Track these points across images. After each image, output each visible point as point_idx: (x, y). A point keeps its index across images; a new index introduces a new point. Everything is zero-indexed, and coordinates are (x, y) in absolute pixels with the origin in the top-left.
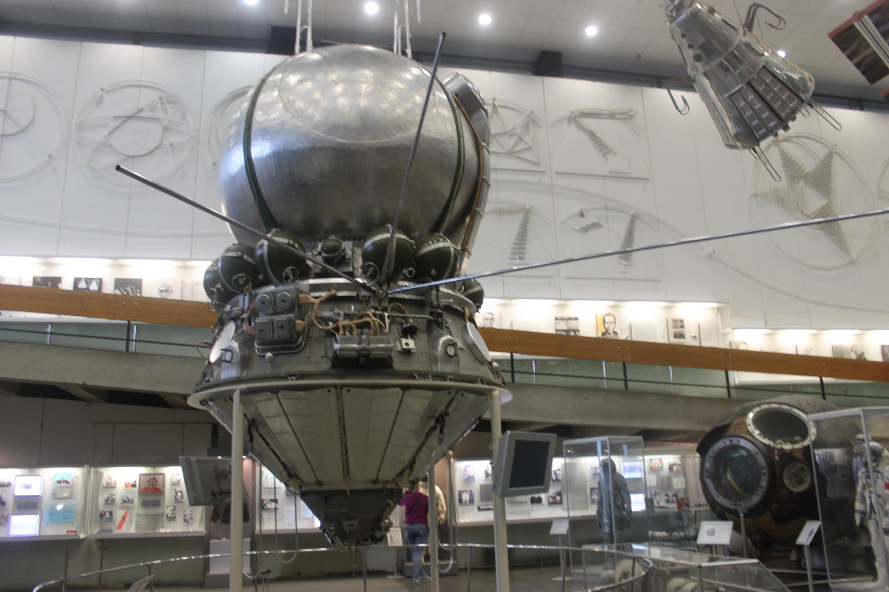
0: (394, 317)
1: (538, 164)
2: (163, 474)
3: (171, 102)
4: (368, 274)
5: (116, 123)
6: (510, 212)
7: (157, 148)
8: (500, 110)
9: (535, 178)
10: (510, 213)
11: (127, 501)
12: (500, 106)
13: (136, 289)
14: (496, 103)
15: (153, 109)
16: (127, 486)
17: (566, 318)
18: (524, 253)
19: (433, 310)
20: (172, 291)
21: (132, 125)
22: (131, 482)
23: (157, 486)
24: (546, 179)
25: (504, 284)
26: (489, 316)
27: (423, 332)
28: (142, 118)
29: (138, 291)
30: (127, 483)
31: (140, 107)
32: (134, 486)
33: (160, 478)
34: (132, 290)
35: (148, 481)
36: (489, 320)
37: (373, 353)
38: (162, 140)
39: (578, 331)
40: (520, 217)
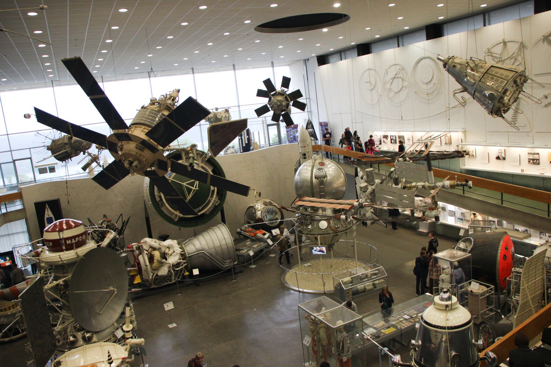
3: (403, 69)
5: (392, 80)
7: (402, 88)
21: (395, 80)
25: (508, 136)
39: (539, 160)
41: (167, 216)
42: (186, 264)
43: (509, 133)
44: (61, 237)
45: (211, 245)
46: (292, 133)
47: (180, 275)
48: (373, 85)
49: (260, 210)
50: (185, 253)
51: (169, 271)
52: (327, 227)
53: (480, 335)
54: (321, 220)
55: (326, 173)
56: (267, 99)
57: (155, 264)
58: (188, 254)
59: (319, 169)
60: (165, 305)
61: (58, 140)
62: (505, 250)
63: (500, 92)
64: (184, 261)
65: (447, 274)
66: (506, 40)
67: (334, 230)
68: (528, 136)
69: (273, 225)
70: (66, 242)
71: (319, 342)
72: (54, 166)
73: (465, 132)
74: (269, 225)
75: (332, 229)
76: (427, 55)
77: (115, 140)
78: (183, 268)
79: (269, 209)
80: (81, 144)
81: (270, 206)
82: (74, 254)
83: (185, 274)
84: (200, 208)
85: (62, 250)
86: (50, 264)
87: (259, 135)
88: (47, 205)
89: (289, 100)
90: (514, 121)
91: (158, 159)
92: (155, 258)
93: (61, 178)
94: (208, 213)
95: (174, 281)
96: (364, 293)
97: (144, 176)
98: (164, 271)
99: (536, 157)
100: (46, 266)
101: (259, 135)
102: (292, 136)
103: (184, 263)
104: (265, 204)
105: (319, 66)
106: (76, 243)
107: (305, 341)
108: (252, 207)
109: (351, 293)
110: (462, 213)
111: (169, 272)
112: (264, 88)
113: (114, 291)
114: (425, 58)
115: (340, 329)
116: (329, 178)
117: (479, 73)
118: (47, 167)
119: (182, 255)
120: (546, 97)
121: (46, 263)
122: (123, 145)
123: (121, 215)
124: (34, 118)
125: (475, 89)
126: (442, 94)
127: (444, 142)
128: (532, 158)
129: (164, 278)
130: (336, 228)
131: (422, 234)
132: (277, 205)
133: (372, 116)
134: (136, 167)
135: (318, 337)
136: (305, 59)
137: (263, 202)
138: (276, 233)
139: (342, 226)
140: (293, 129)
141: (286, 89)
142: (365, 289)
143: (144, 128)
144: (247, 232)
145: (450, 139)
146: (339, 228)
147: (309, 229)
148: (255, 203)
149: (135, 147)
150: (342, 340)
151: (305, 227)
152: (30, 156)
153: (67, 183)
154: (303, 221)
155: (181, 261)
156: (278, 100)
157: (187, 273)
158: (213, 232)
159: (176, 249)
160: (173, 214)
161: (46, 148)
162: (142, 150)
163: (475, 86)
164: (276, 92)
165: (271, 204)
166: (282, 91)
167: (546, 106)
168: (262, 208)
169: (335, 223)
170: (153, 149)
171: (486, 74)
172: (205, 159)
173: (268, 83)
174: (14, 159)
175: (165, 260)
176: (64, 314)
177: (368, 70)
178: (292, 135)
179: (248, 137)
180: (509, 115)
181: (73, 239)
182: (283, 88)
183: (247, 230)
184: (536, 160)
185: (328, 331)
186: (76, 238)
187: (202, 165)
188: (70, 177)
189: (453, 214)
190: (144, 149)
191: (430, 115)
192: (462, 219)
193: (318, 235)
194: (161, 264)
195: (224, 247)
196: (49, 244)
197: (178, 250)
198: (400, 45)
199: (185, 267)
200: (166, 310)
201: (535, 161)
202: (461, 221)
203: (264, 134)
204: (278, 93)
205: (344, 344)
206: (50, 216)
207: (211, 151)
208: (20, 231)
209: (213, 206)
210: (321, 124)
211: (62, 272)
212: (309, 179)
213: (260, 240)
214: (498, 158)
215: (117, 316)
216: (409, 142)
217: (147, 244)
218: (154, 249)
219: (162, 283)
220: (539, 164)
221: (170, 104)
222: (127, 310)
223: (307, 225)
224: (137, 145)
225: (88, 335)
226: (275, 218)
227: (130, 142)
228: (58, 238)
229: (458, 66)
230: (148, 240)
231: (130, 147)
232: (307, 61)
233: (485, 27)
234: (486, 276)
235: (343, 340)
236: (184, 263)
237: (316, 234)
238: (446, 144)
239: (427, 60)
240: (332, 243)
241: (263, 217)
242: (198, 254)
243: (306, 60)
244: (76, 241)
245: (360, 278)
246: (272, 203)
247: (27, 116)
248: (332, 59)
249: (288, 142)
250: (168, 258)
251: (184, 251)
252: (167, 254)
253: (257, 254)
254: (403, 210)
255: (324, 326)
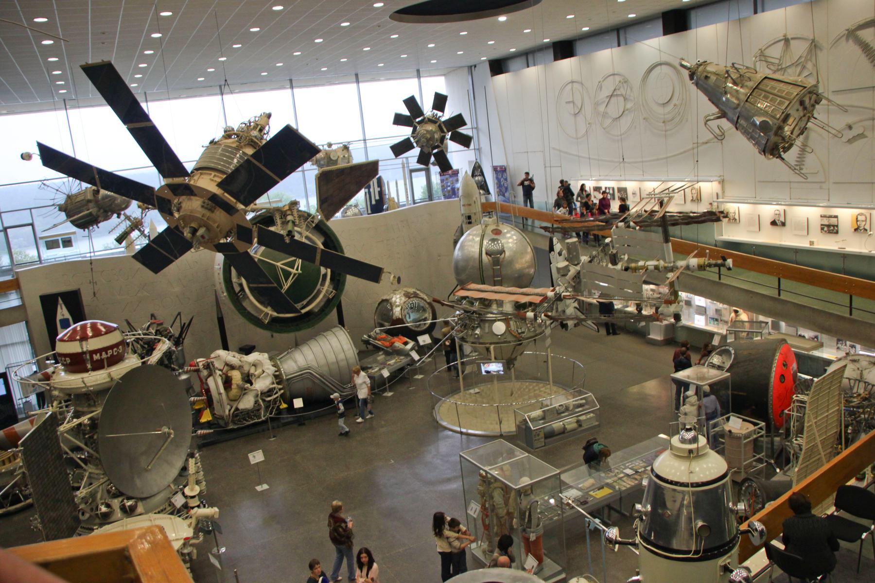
3: (625, 82)
7: (623, 112)
21: (613, 100)
25: (790, 188)
26: (777, 212)
38: (625, 107)
39: (837, 226)
41: (252, 315)
42: (282, 391)
43: (791, 184)
44: (85, 349)
45: (322, 361)
46: (449, 184)
47: (273, 408)
48: (577, 107)
49: (399, 306)
50: (281, 374)
51: (256, 402)
52: (505, 332)
53: (743, 498)
54: (495, 321)
55: (503, 246)
56: (410, 129)
57: (234, 391)
58: (286, 376)
59: (493, 240)
60: (250, 456)
61: (77, 195)
62: (784, 367)
63: (779, 119)
64: (280, 387)
65: (693, 405)
66: (789, 37)
67: (515, 336)
68: (821, 188)
69: (419, 329)
70: (92, 358)
71: (493, 511)
72: (70, 238)
73: (722, 182)
74: (413, 328)
75: (513, 335)
76: (665, 58)
77: (168, 195)
78: (277, 397)
79: (413, 303)
80: (115, 200)
81: (414, 299)
82: (105, 375)
83: (281, 407)
84: (305, 302)
85: (86, 370)
86: (68, 392)
87: (397, 187)
88: (60, 299)
89: (445, 130)
90: (800, 165)
91: (237, 225)
92: (234, 382)
93: (82, 255)
94: (316, 310)
95: (263, 419)
96: (563, 435)
97: (213, 251)
98: (247, 403)
99: (833, 221)
100: (61, 395)
101: (397, 187)
102: (449, 188)
103: (280, 389)
104: (408, 295)
105: (492, 76)
106: (107, 358)
107: (471, 510)
108: (387, 301)
109: (543, 436)
110: (717, 311)
111: (256, 404)
112: (406, 112)
113: (169, 434)
114: (661, 64)
115: (526, 491)
116: (507, 254)
117: (745, 88)
118: (59, 238)
119: (276, 376)
120: (850, 127)
121: (61, 390)
122: (181, 203)
123: (179, 314)
124: (37, 159)
125: (739, 113)
126: (687, 121)
127: (689, 198)
128: (827, 223)
129: (248, 413)
130: (519, 334)
131: (653, 343)
132: (426, 297)
133: (576, 156)
134: (203, 237)
135: (491, 503)
136: (470, 64)
137: (403, 292)
138: (424, 341)
139: (529, 330)
140: (451, 177)
141: (440, 114)
142: (565, 428)
143: (215, 176)
144: (379, 340)
145: (699, 192)
146: (523, 333)
147: (476, 334)
148: (392, 295)
149: (200, 206)
150: (528, 507)
151: (470, 332)
152: (31, 222)
153: (91, 263)
154: (467, 322)
155: (275, 385)
156: (427, 131)
157: (284, 406)
158: (326, 340)
159: (266, 367)
160: (262, 311)
161: (58, 208)
162: (211, 210)
163: (739, 109)
164: (425, 118)
165: (416, 296)
166: (434, 116)
167: (850, 141)
168: (402, 302)
169: (517, 324)
170: (229, 209)
171: (756, 90)
172: (311, 225)
173: (411, 103)
174: (6, 225)
175: (249, 385)
176: (90, 470)
177: (570, 83)
178: (449, 186)
179: (379, 189)
180: (791, 155)
181: (104, 353)
182: (435, 112)
183: (378, 336)
184: (834, 226)
185: (507, 494)
186: (109, 351)
187: (308, 234)
188: (96, 254)
189: (702, 311)
190: (215, 209)
191: (669, 155)
192: (717, 320)
193: (491, 344)
194: (243, 391)
195: (343, 364)
196: (65, 361)
197: (270, 369)
198: (622, 42)
199: (282, 395)
200: (252, 463)
201: (832, 228)
202: (716, 322)
203: (405, 184)
204: (427, 119)
205: (532, 513)
206: (65, 317)
207: (321, 213)
208: (17, 341)
209: (325, 299)
210: (495, 169)
211: (87, 404)
212: (477, 255)
213: (399, 352)
214: (774, 223)
215: (174, 472)
216: (634, 197)
217: (220, 359)
218: (232, 367)
219: (245, 422)
220: (837, 232)
221: (256, 137)
222: (190, 463)
223: (474, 329)
224: (204, 203)
225: (129, 503)
226: (423, 317)
227: (192, 197)
228: (80, 350)
229: (713, 78)
230: (221, 353)
231: (193, 205)
232: (473, 68)
233: (756, 15)
234: (754, 407)
235: (530, 508)
236: (280, 389)
237: (487, 343)
238: (692, 200)
239: (663, 67)
240: (513, 357)
241: (403, 317)
242: (302, 374)
243: (471, 67)
244: (109, 355)
245: (557, 411)
246: (418, 294)
247: (26, 157)
248: (513, 65)
249: (443, 197)
250: (253, 381)
251: (279, 370)
252: (252, 375)
253: (393, 375)
254: (625, 304)
255: (500, 486)
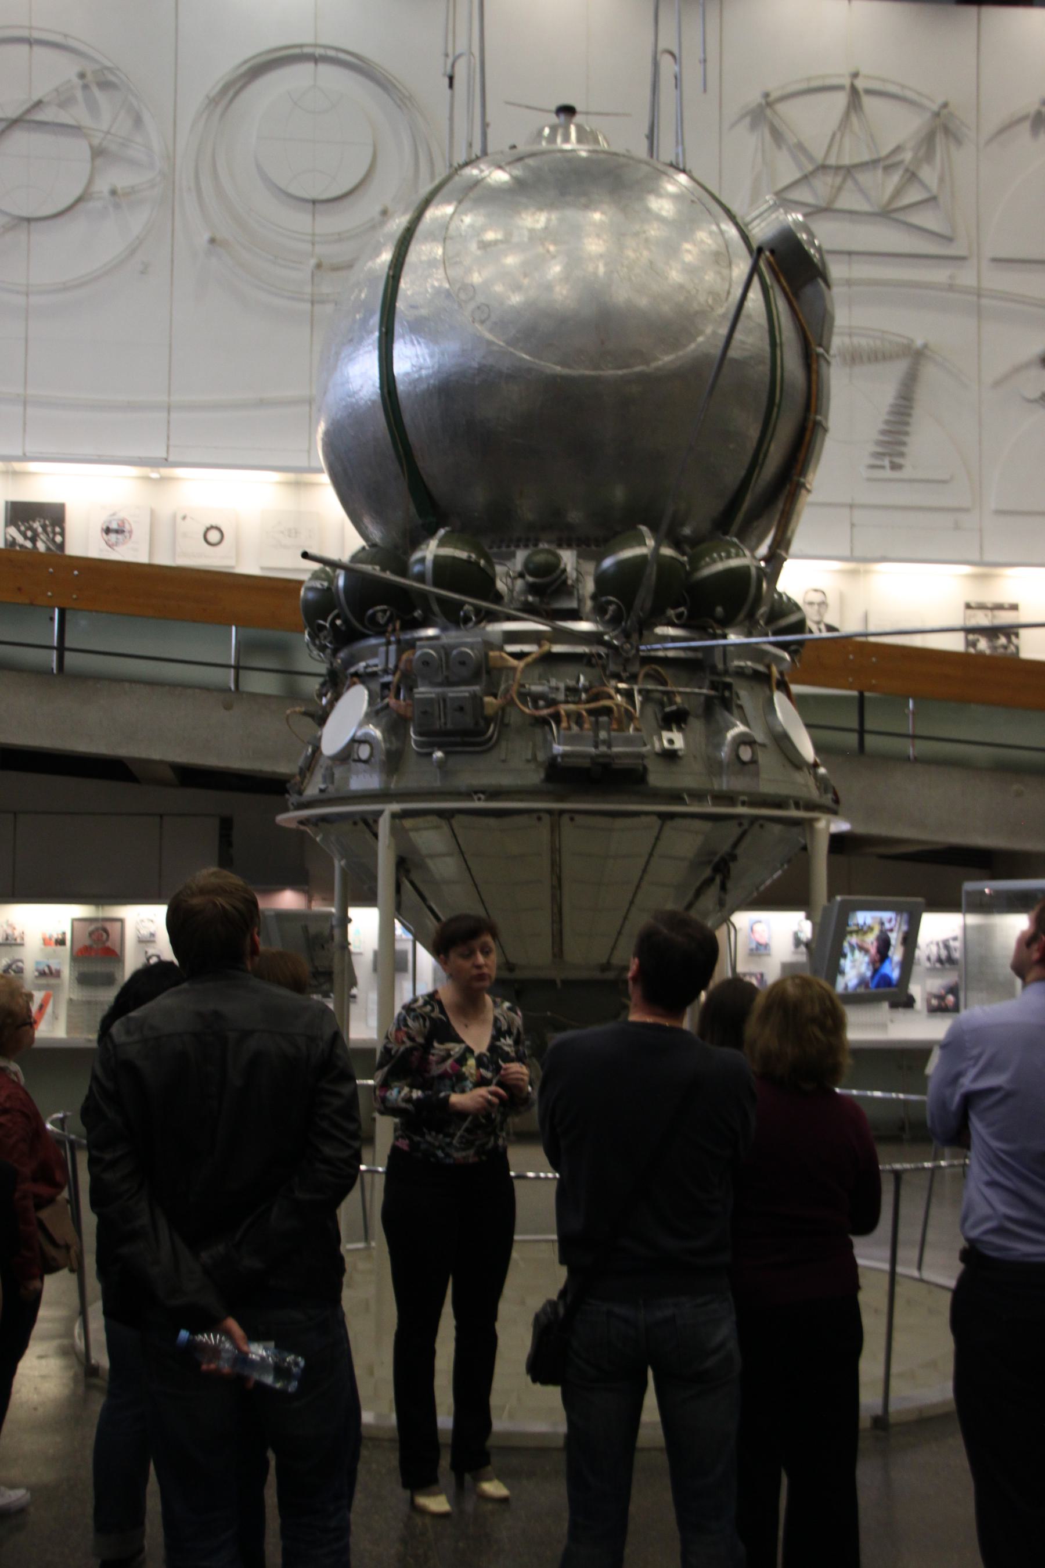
0: (648, 691)
1: (949, 239)
2: (121, 921)
3: (105, 85)
4: (607, 617)
6: (877, 356)
7: (79, 200)
8: (867, 101)
9: (939, 275)
10: (876, 359)
11: (48, 974)
12: (869, 92)
13: (53, 525)
14: (860, 84)
15: (65, 102)
16: (46, 942)
17: (989, 605)
18: (902, 455)
19: (716, 678)
20: (131, 532)
22: (56, 934)
23: (109, 944)
24: (966, 277)
25: (853, 525)
27: (697, 717)
28: (42, 125)
29: (58, 530)
30: (48, 936)
31: (35, 98)
32: (61, 942)
33: (114, 929)
34: (44, 527)
35: (91, 934)
36: (816, 607)
37: (617, 761)
38: (90, 181)
40: (899, 368)
68: (957, 527)
